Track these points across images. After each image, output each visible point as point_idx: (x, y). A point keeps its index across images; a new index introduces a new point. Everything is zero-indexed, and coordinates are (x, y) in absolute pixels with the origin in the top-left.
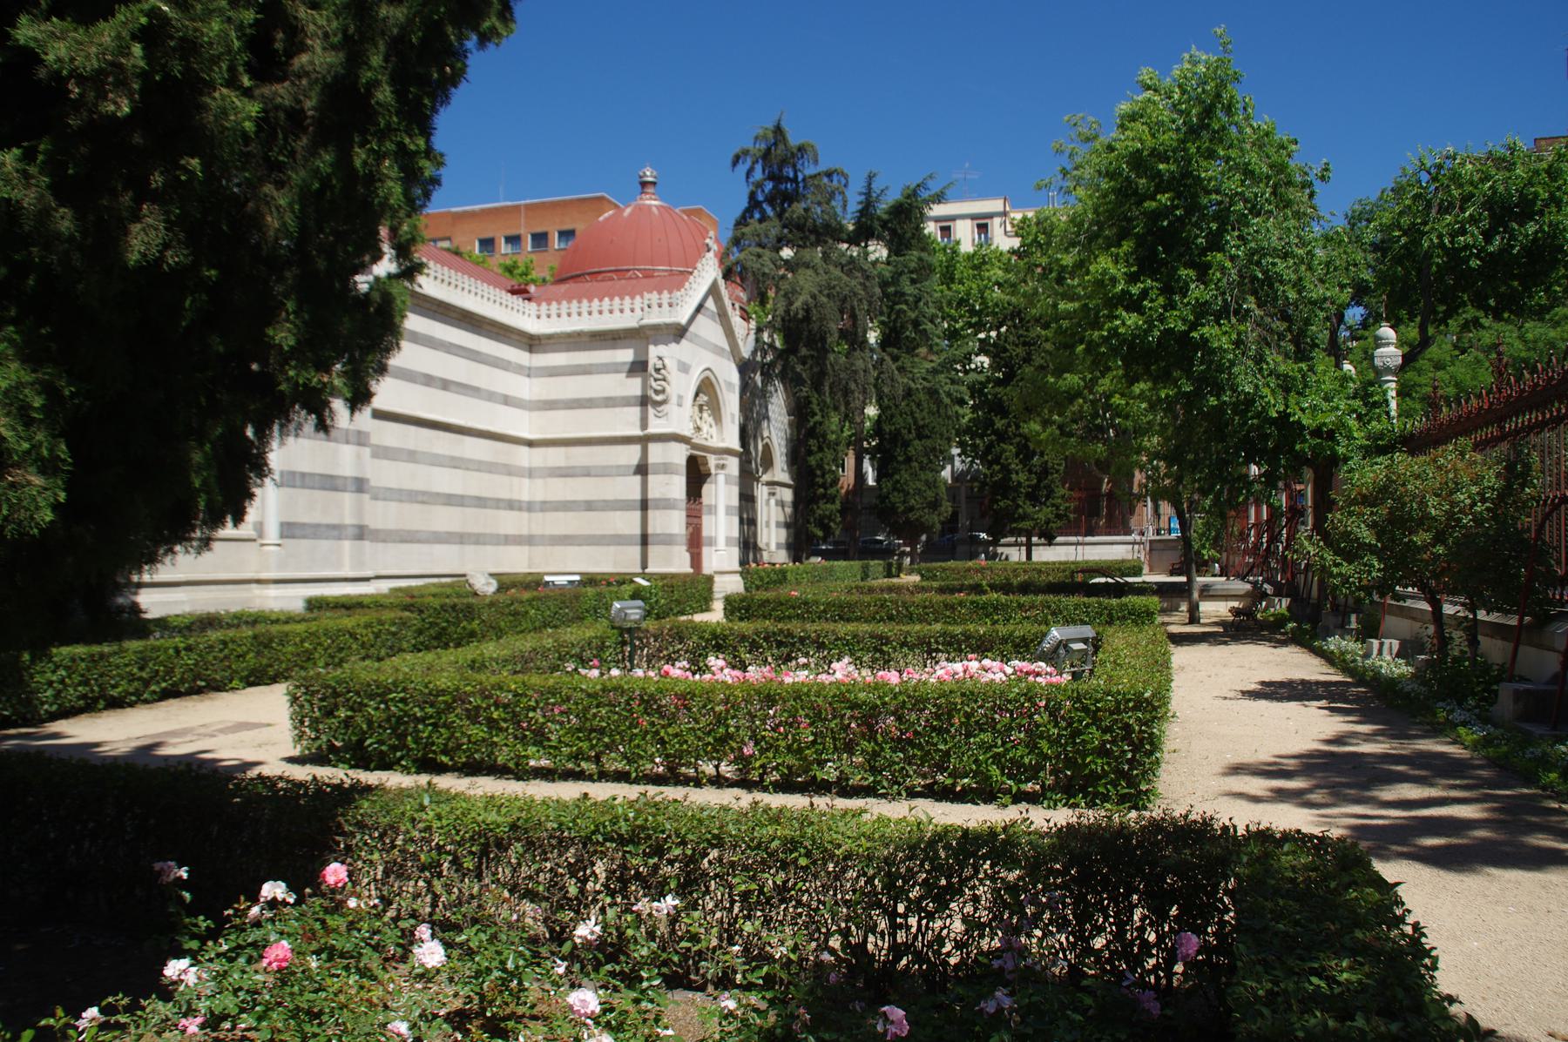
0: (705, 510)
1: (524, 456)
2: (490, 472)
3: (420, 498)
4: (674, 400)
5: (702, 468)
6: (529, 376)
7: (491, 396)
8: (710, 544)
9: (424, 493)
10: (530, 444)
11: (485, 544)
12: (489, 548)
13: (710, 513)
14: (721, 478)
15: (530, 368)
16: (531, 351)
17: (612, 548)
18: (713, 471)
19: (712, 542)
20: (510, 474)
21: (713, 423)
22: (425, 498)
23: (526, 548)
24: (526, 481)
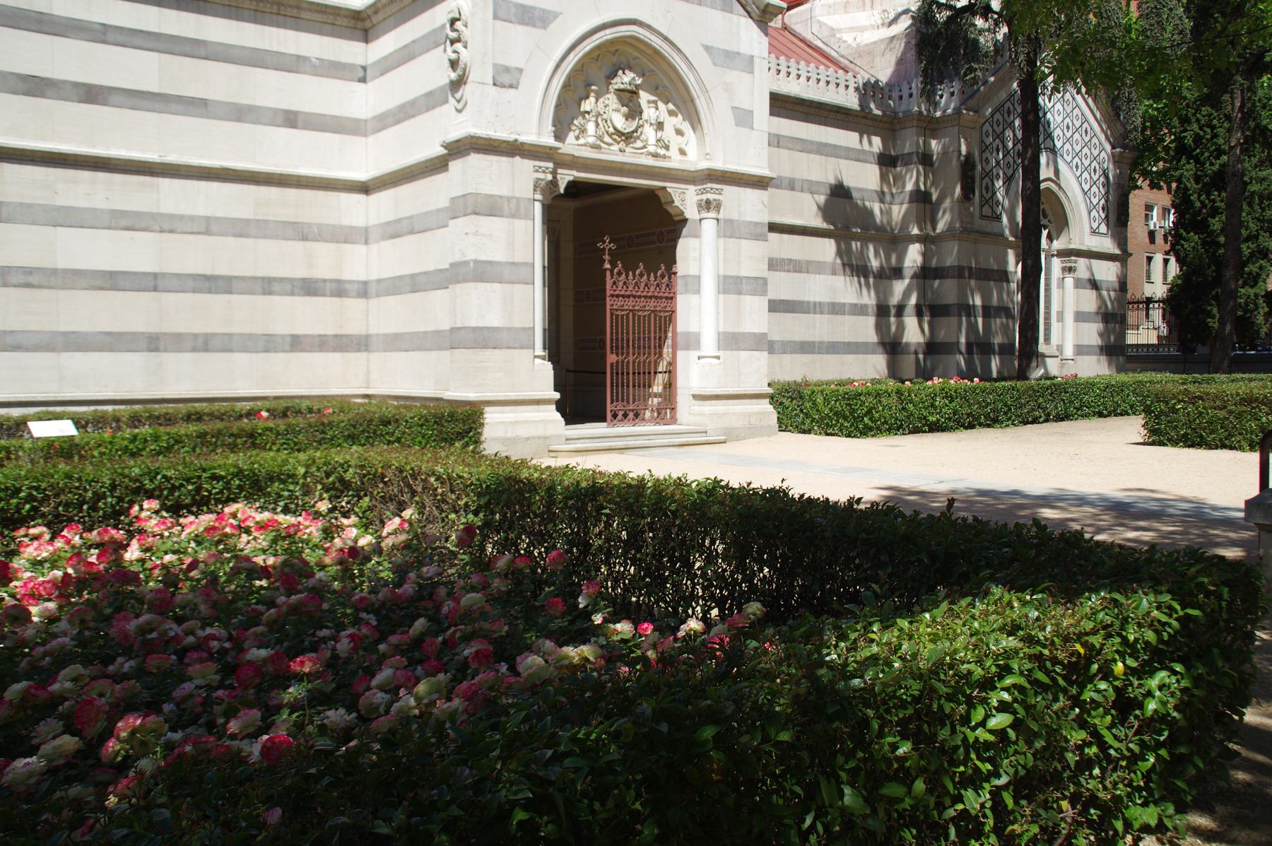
0: (680, 284)
1: (353, 210)
2: (241, 235)
3: (21, 279)
4: (480, 74)
5: (670, 210)
6: (363, 80)
7: (241, 113)
8: (687, 348)
9: (29, 271)
10: (364, 188)
11: (231, 351)
12: (241, 358)
13: (687, 291)
14: (709, 227)
15: (364, 68)
16: (366, 40)
17: (434, 354)
18: (691, 212)
19: (693, 342)
20: (305, 238)
21: (686, 127)
22: (33, 280)
23: (364, 355)
24: (360, 249)
